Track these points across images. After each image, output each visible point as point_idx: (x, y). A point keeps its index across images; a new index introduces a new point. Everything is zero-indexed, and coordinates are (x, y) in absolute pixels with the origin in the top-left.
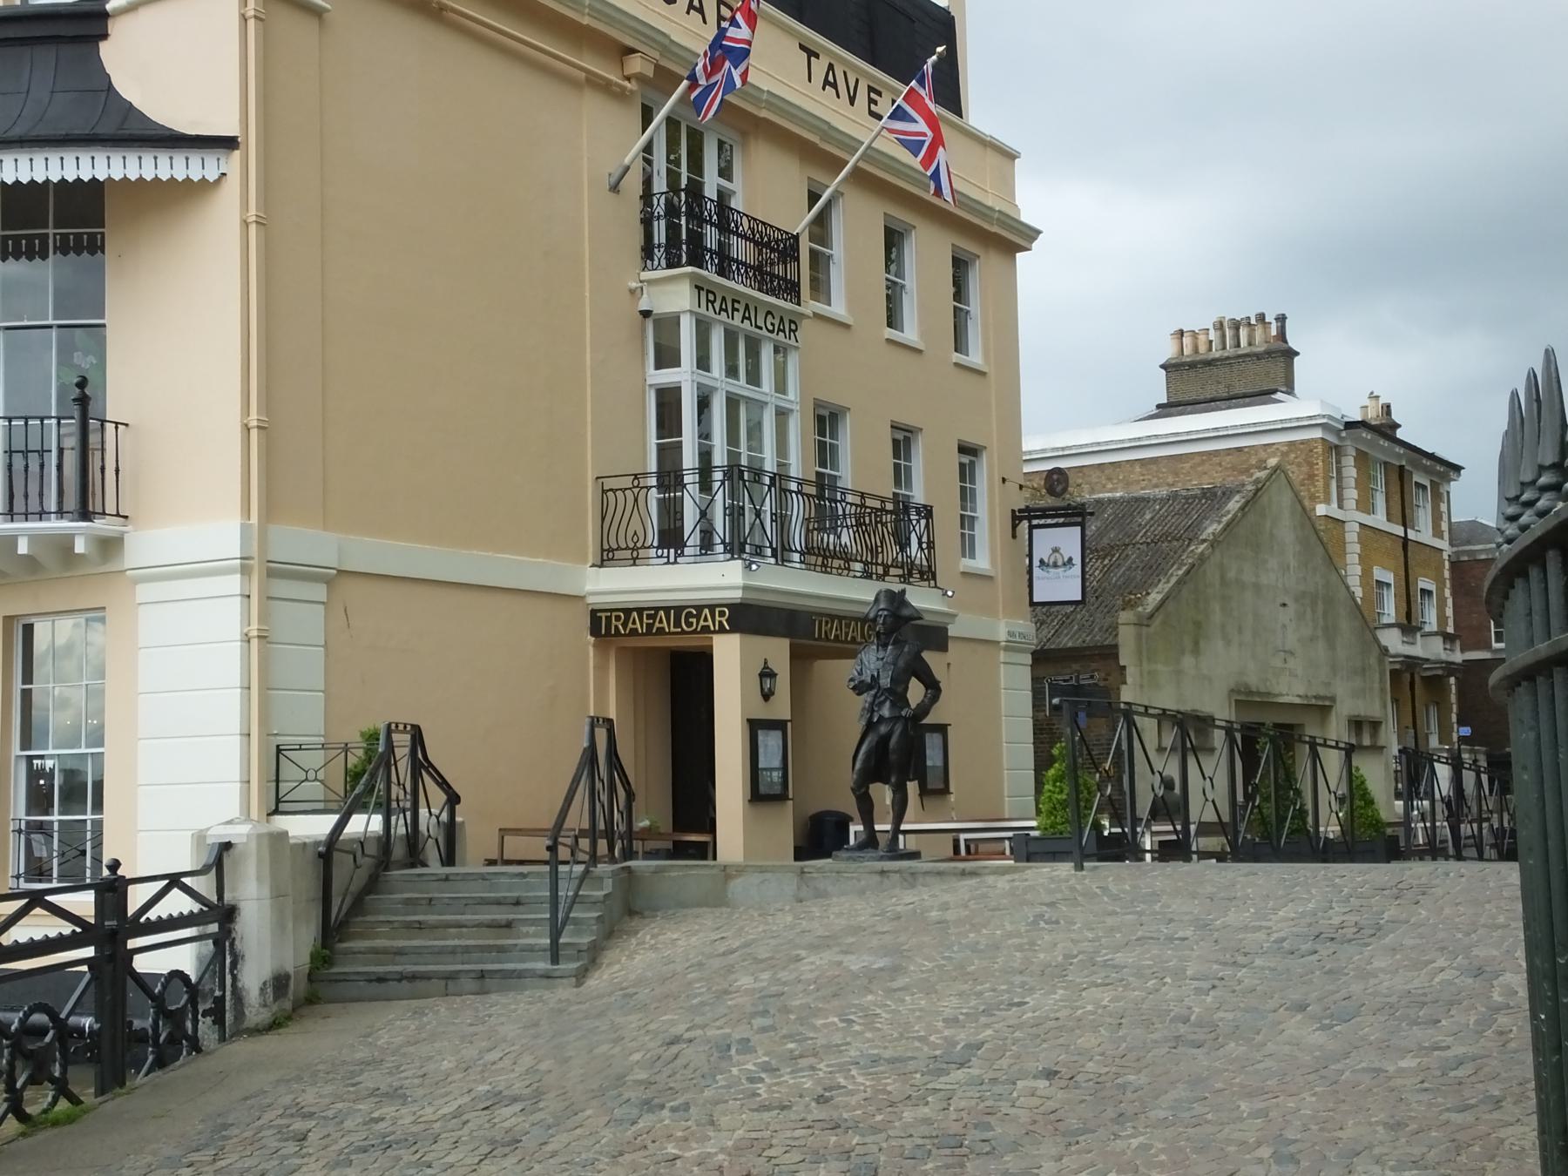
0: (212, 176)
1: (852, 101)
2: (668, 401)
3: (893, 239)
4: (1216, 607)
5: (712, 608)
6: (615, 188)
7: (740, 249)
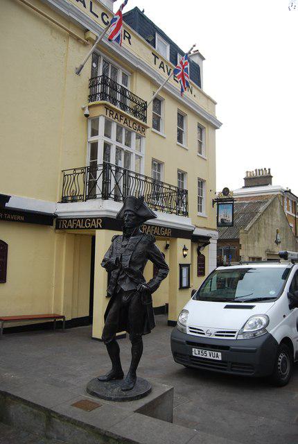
1: (169, 74)
2: (94, 146)
3: (181, 118)
4: (263, 229)
5: (96, 219)
6: (78, 73)
7: (129, 103)
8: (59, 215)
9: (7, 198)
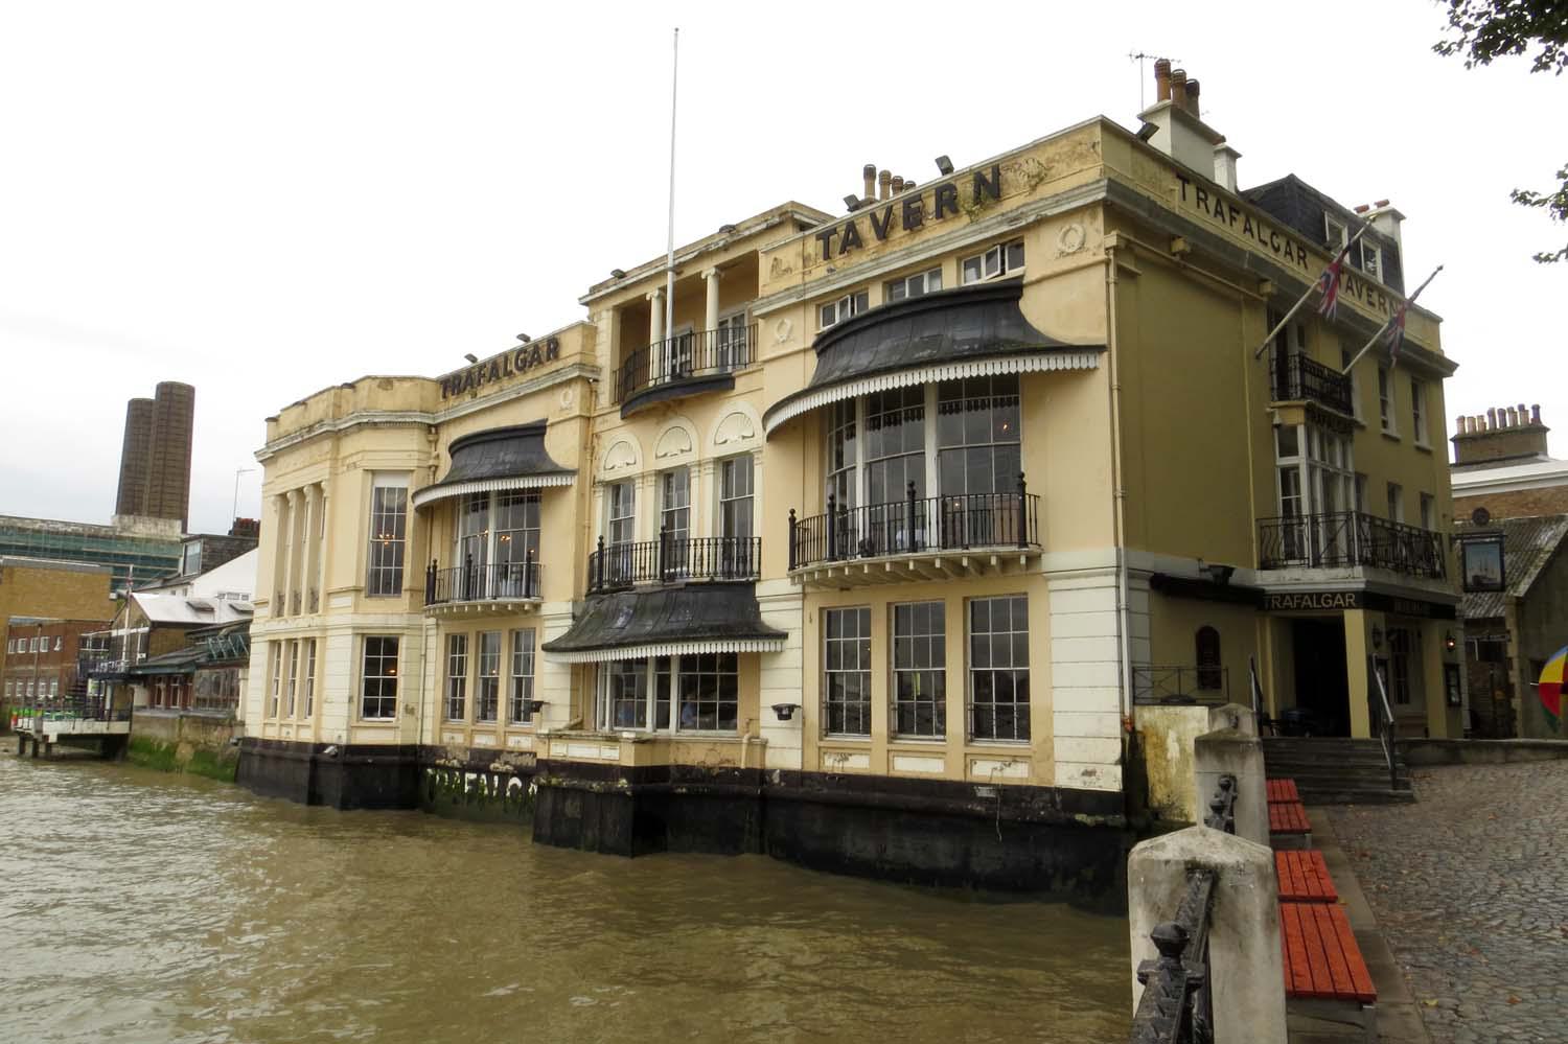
0: (1092, 366)
1: (1360, 296)
5: (1343, 594)
6: (1258, 357)
8: (1267, 588)
9: (1228, 571)
